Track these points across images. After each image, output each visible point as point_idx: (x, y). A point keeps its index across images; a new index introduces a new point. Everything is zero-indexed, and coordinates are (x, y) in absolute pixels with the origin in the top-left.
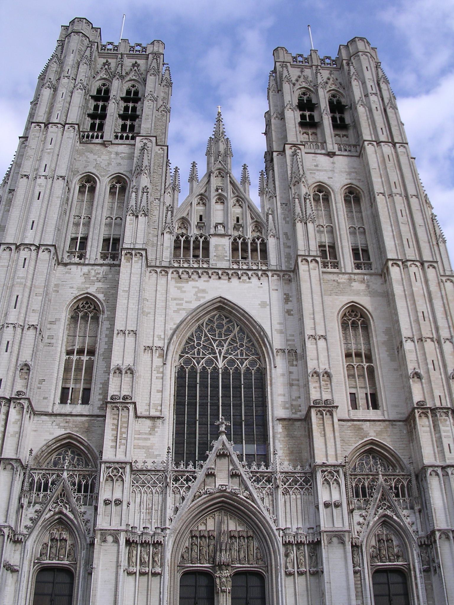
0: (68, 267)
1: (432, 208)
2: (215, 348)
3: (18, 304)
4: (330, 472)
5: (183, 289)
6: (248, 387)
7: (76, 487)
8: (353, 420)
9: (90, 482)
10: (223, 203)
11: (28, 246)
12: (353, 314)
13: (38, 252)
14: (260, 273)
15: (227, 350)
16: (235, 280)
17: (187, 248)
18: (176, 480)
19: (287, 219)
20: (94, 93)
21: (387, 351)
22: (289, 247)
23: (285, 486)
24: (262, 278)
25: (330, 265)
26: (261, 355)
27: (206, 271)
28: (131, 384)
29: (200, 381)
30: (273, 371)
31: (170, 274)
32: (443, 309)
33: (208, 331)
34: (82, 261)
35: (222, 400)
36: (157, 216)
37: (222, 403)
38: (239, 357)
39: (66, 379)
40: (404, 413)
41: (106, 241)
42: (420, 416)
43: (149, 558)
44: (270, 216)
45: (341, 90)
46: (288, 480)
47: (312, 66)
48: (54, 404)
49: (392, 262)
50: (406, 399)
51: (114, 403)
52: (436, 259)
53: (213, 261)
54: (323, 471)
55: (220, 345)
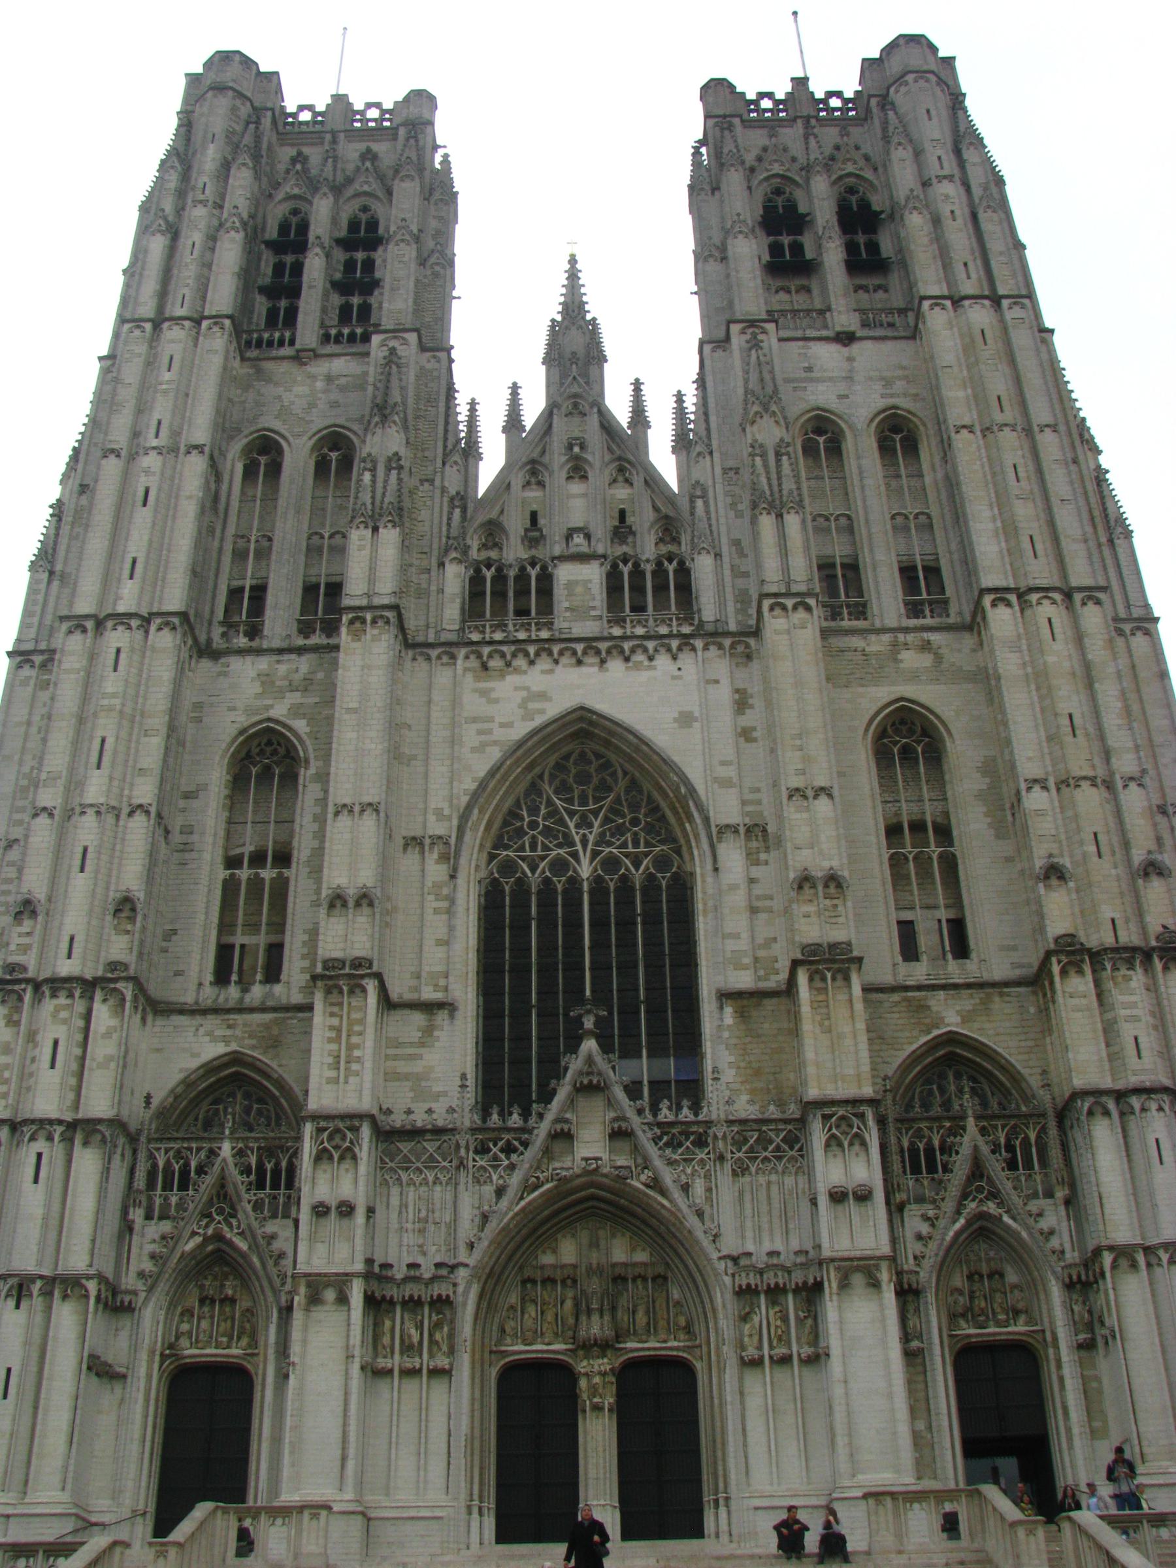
0: (223, 660)
1: (1100, 452)
2: (573, 831)
4: (843, 1118)
5: (494, 695)
7: (253, 1177)
8: (906, 988)
9: (284, 1164)
10: (584, 477)
11: (122, 619)
12: (904, 728)
13: (147, 632)
14: (675, 644)
16: (616, 666)
17: (499, 595)
18: (482, 1150)
19: (740, 507)
20: (272, 233)
21: (986, 815)
22: (746, 575)
23: (740, 1154)
24: (681, 656)
25: (845, 611)
26: (682, 841)
27: (544, 648)
29: (539, 913)
30: (710, 880)
31: (459, 662)
32: (1119, 705)
33: (556, 792)
34: (254, 644)
35: (591, 955)
36: (427, 524)
37: (592, 962)
38: (631, 850)
39: (225, 925)
40: (1030, 966)
41: (310, 590)
42: (1064, 972)
43: (422, 1334)
44: (699, 503)
45: (868, 174)
46: (746, 1140)
48: (200, 984)
49: (992, 596)
50: (1034, 930)
51: (330, 978)
52: (1108, 579)
53: (565, 622)
54: (826, 1118)
55: (584, 823)
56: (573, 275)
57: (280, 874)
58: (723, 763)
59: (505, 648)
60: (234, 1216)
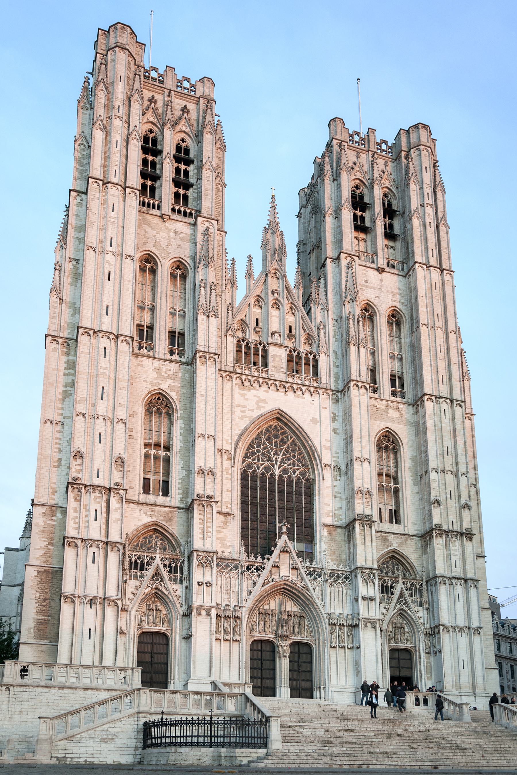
0: (140, 359)
3: (104, 396)
5: (246, 397)
6: (299, 494)
10: (278, 308)
15: (282, 459)
16: (290, 393)
19: (337, 337)
24: (313, 395)
28: (213, 485)
30: (321, 483)
31: (234, 380)
34: (151, 353)
44: (322, 331)
47: (368, 151)
56: (274, 207)
57: (166, 454)
58: (326, 440)
59: (250, 378)
60: (162, 580)
